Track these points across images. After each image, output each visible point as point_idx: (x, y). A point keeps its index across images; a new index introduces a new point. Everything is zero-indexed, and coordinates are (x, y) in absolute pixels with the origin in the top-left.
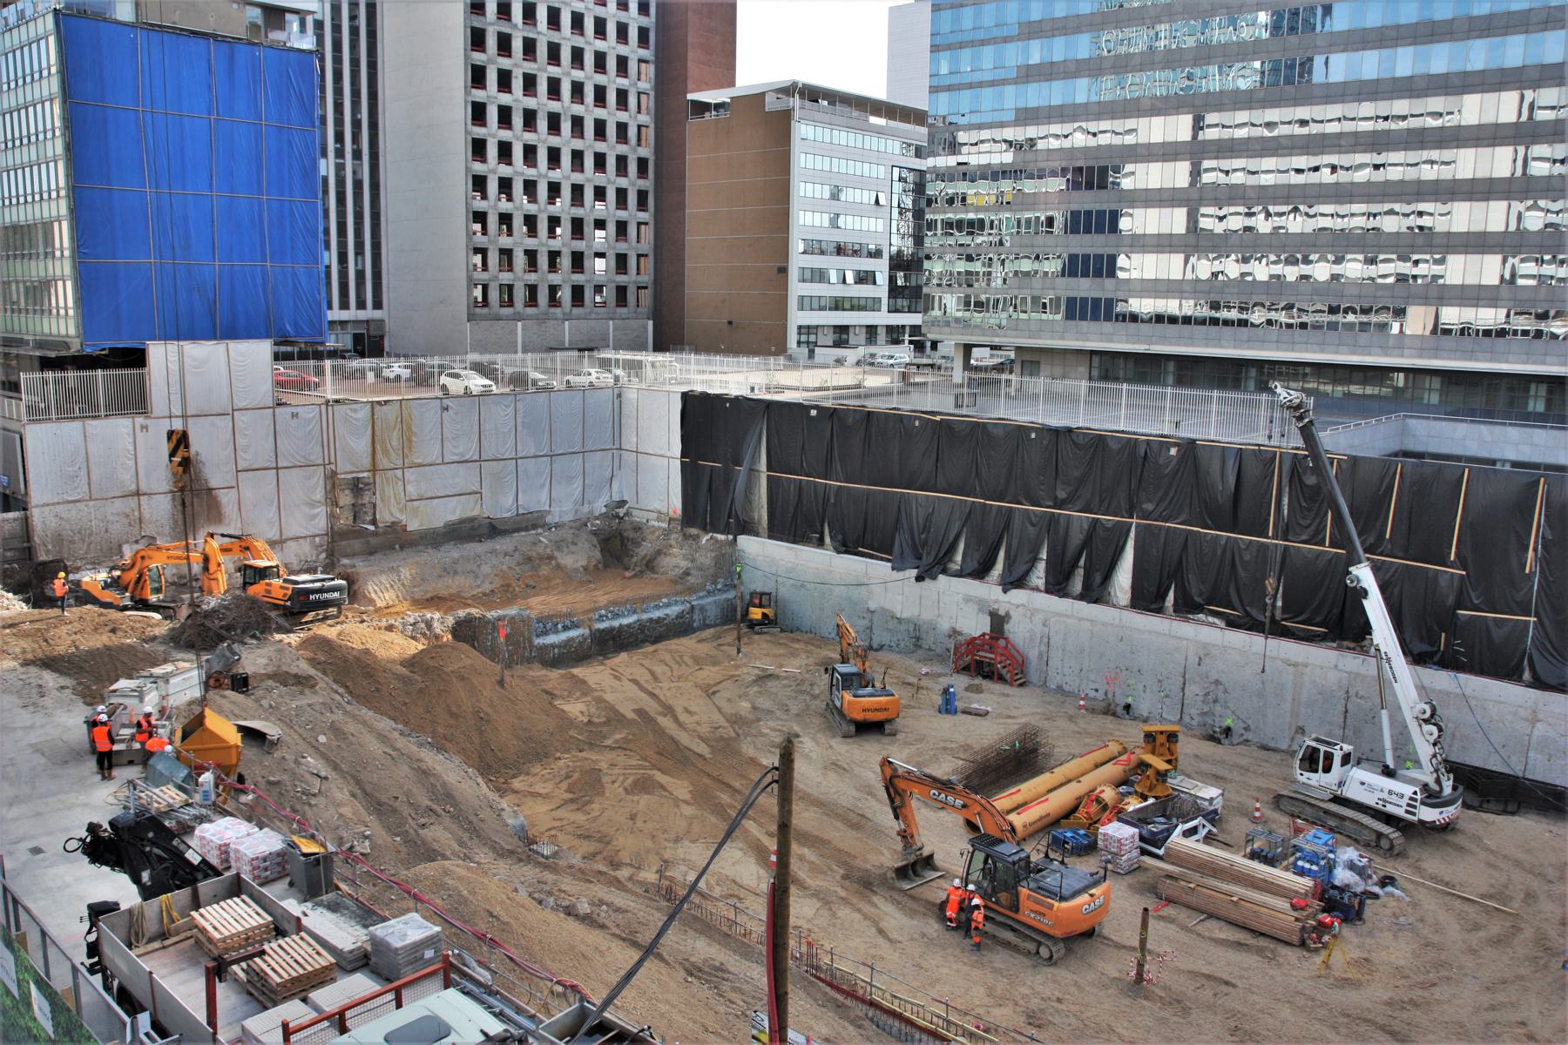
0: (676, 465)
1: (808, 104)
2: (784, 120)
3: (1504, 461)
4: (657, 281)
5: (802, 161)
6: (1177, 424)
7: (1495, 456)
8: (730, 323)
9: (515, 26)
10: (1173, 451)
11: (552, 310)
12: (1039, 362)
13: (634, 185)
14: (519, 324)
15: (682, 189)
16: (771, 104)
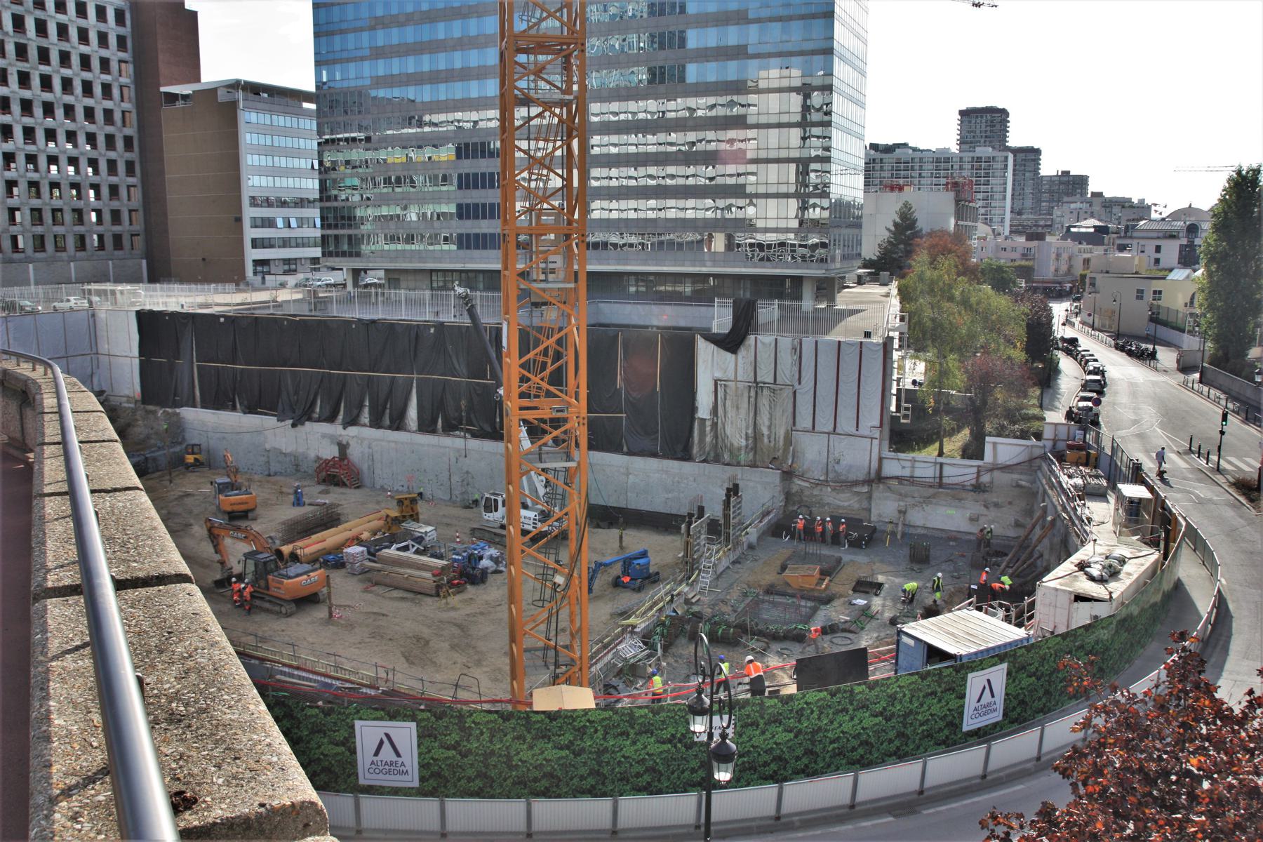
0: (136, 362)
1: (251, 96)
2: (233, 106)
3: (652, 327)
4: (148, 230)
5: (248, 138)
6: (437, 314)
7: (647, 323)
8: (204, 259)
9: (7, 34)
10: (432, 330)
11: (59, 254)
12: (398, 280)
13: (122, 157)
14: (31, 266)
15: (161, 160)
16: (222, 96)
